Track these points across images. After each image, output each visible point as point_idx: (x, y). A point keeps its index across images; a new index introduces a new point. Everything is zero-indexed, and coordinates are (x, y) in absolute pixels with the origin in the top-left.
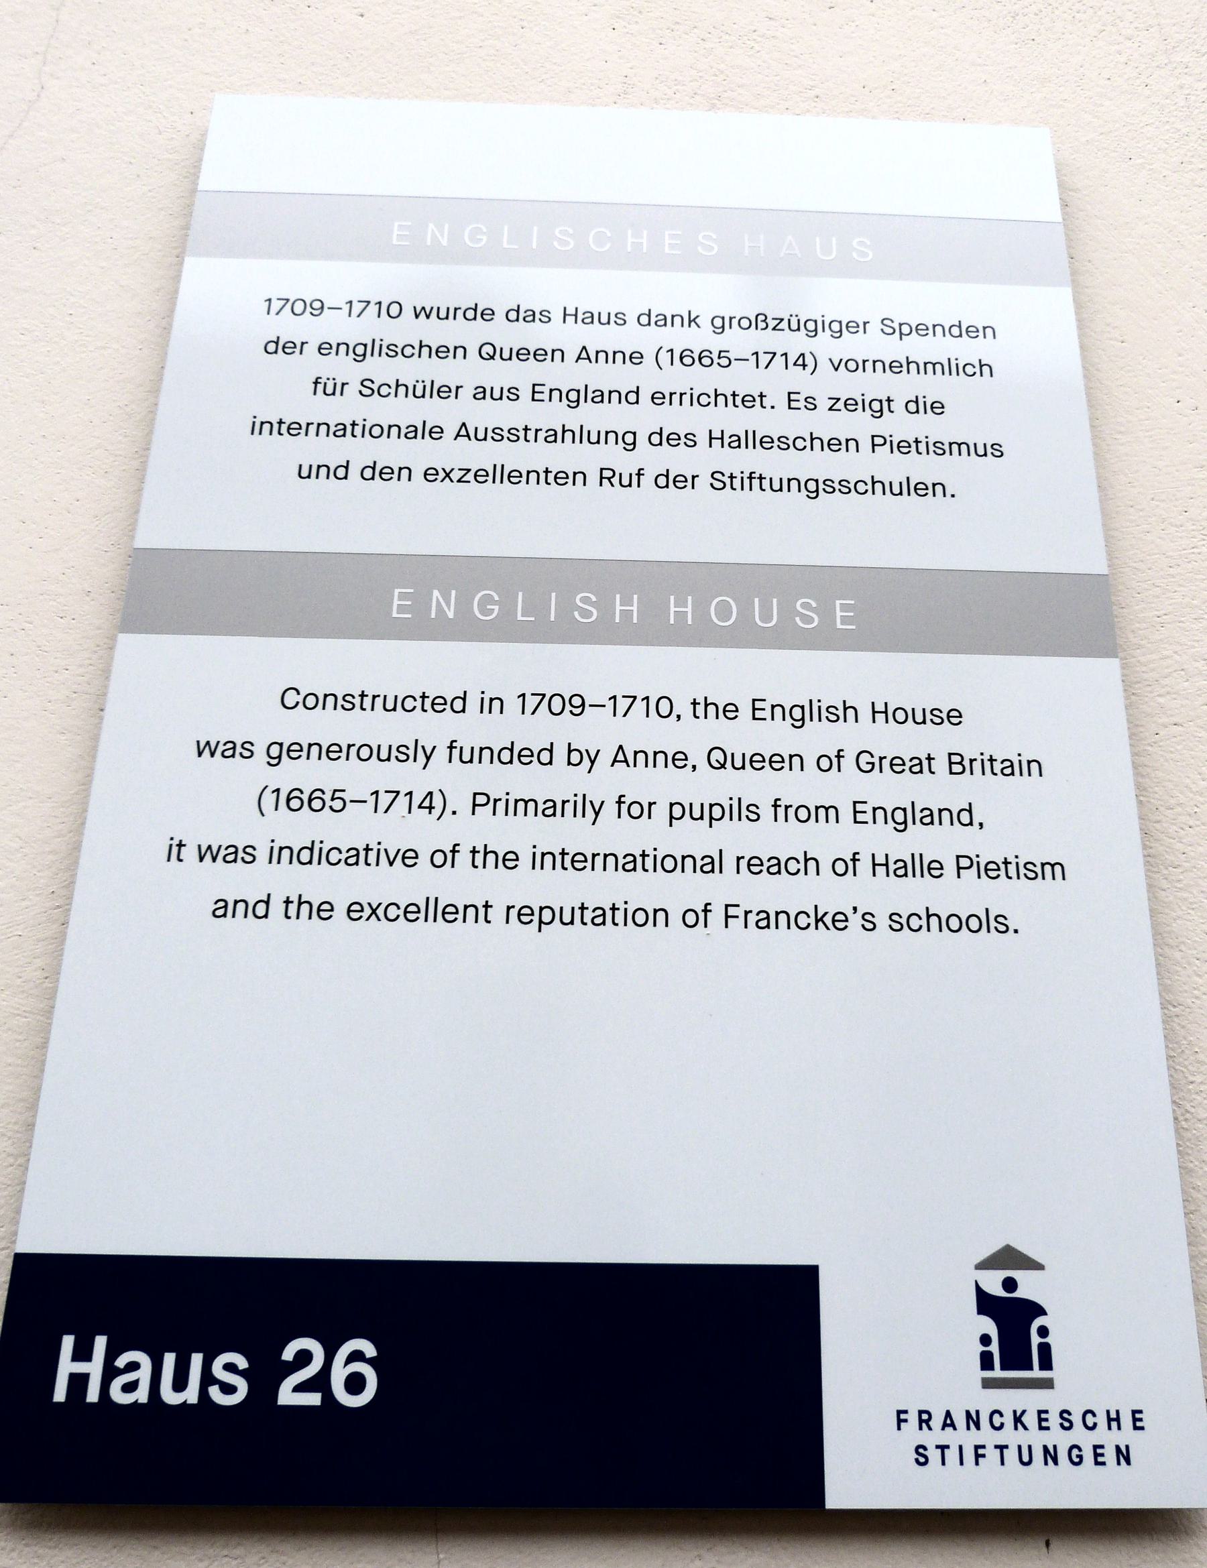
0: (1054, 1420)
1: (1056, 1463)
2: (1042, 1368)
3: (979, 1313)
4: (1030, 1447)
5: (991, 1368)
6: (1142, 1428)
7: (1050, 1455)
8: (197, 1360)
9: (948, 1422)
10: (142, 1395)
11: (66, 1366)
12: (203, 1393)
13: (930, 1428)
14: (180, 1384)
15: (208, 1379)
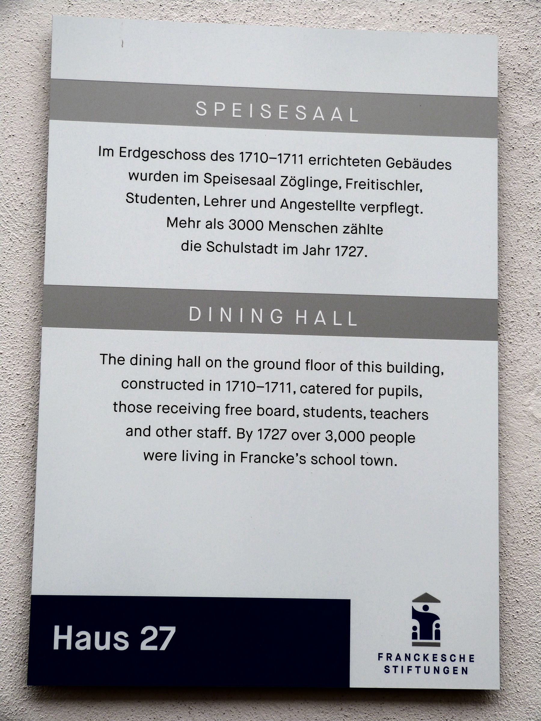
0: (439, 658)
1: (438, 673)
2: (436, 639)
3: (413, 618)
4: (429, 667)
5: (416, 639)
6: (473, 661)
7: (437, 670)
8: (108, 634)
9: (398, 658)
10: (88, 647)
11: (57, 637)
13: (391, 660)
14: (102, 643)
15: (113, 641)
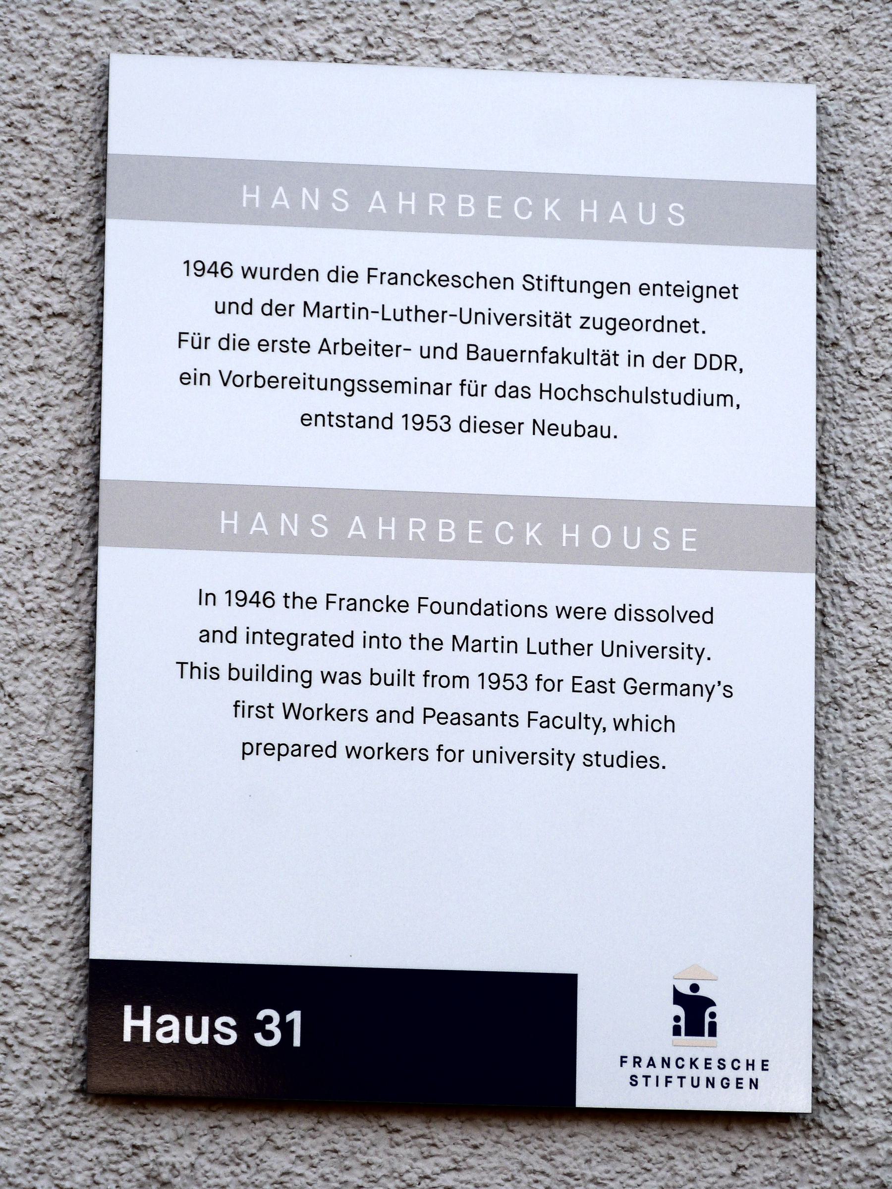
0: (714, 1064)
7: (710, 1083)
8: (205, 1020)
9: (651, 1063)
10: (175, 1038)
11: (129, 1023)
12: (211, 1038)
14: (197, 1032)
15: (213, 1031)
